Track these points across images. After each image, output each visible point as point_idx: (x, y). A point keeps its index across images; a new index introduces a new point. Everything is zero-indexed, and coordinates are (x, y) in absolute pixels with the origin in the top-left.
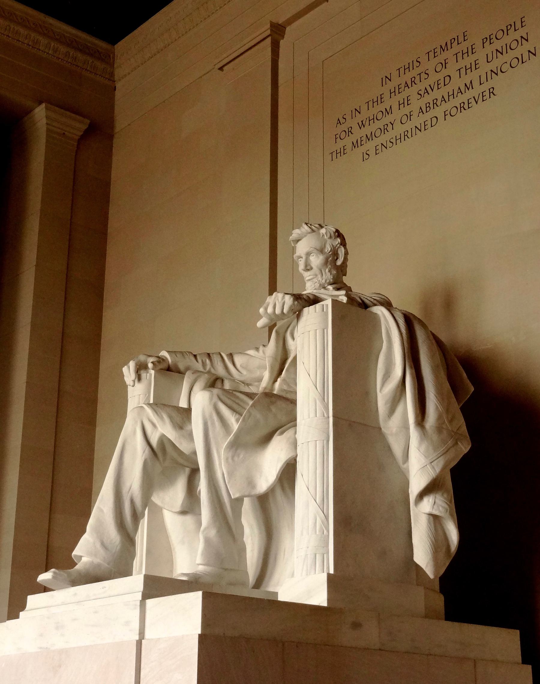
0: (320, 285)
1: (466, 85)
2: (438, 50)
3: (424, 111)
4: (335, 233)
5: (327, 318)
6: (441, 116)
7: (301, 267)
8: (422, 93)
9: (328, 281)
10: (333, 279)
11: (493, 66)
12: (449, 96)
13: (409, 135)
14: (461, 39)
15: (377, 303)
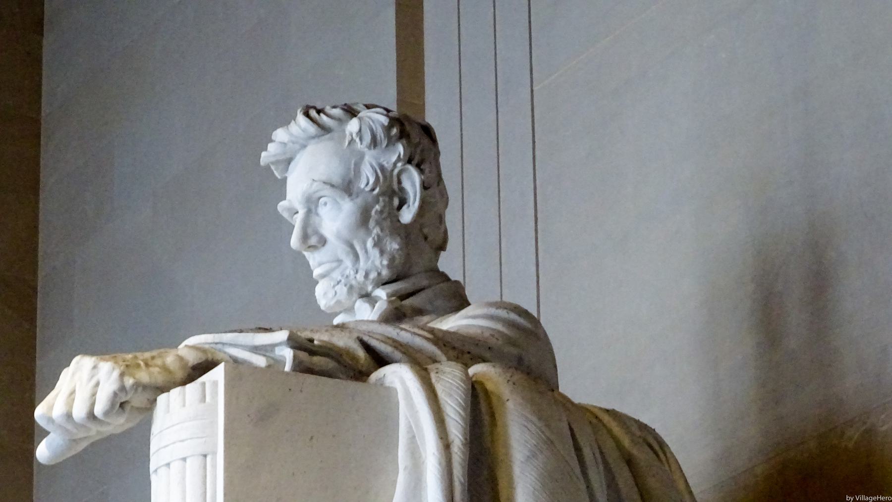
0: (351, 288)
4: (388, 129)
5: (214, 423)
7: (295, 241)
9: (373, 275)
10: (389, 266)
15: (397, 355)
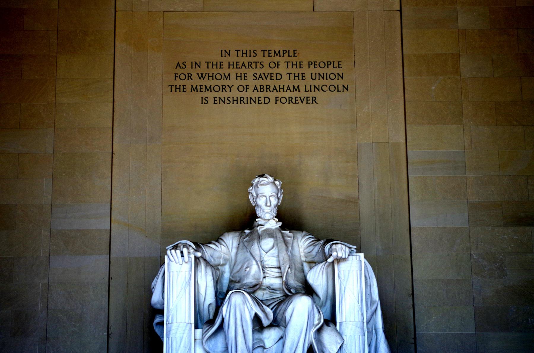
1: (294, 87)
2: (273, 52)
3: (259, 90)
6: (273, 100)
12: (280, 88)
13: (245, 101)
14: (292, 53)
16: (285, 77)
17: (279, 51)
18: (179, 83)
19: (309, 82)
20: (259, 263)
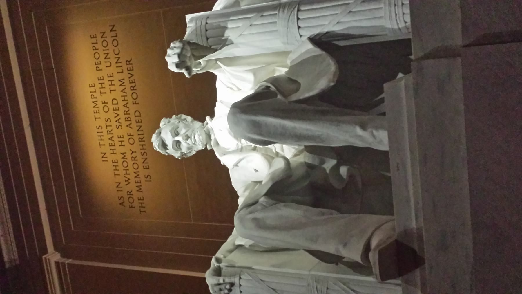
2: (95, 109)
8: (118, 124)
11: (113, 61)
12: (125, 100)
13: (141, 137)
14: (92, 89)
16: (113, 95)
17: (93, 102)
18: (136, 204)
19: (113, 70)
20: (241, 157)
